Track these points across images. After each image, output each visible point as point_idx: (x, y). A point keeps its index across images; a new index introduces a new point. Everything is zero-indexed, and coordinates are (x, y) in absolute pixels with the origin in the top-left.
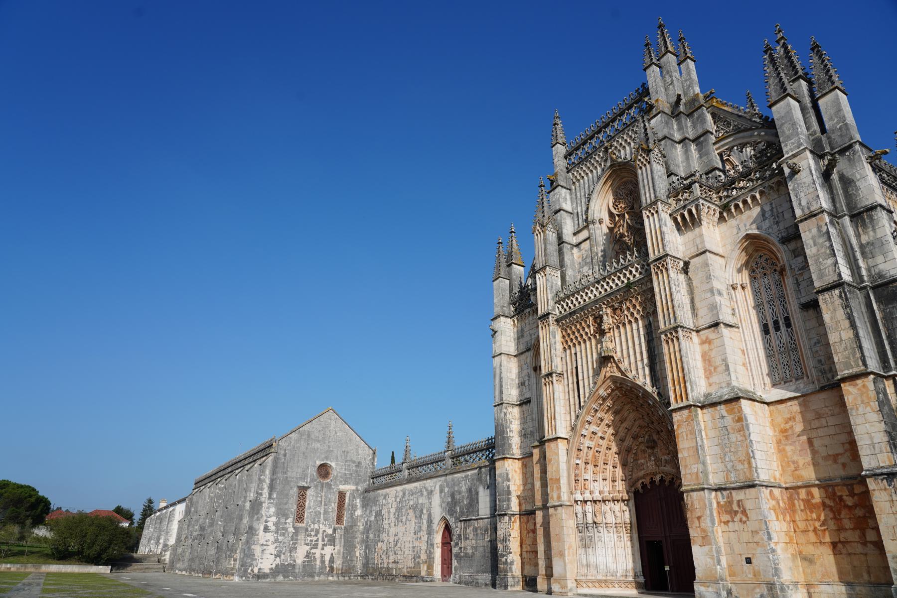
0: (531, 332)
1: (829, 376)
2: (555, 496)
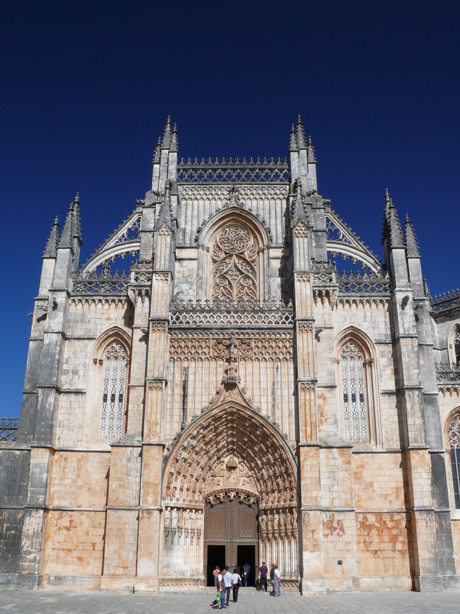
0: (98, 321)
1: (391, 443)
2: (150, 499)
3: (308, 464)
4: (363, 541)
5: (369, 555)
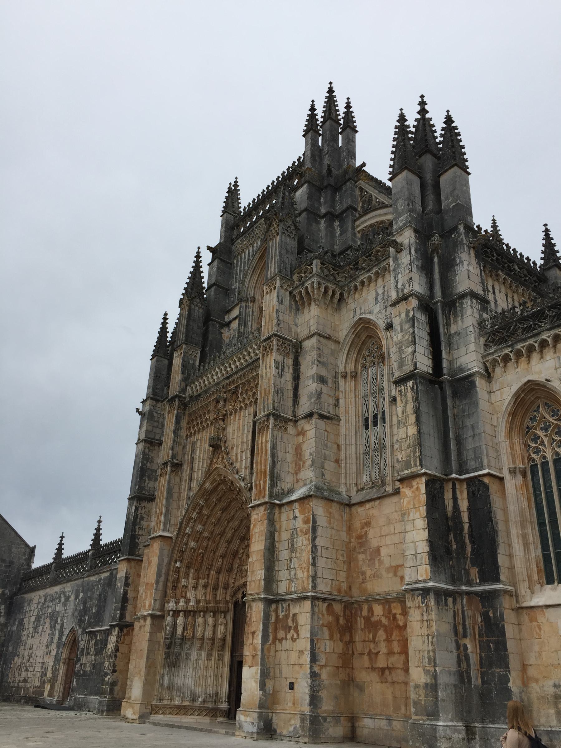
3: (256, 533)
4: (368, 650)
5: (374, 677)
